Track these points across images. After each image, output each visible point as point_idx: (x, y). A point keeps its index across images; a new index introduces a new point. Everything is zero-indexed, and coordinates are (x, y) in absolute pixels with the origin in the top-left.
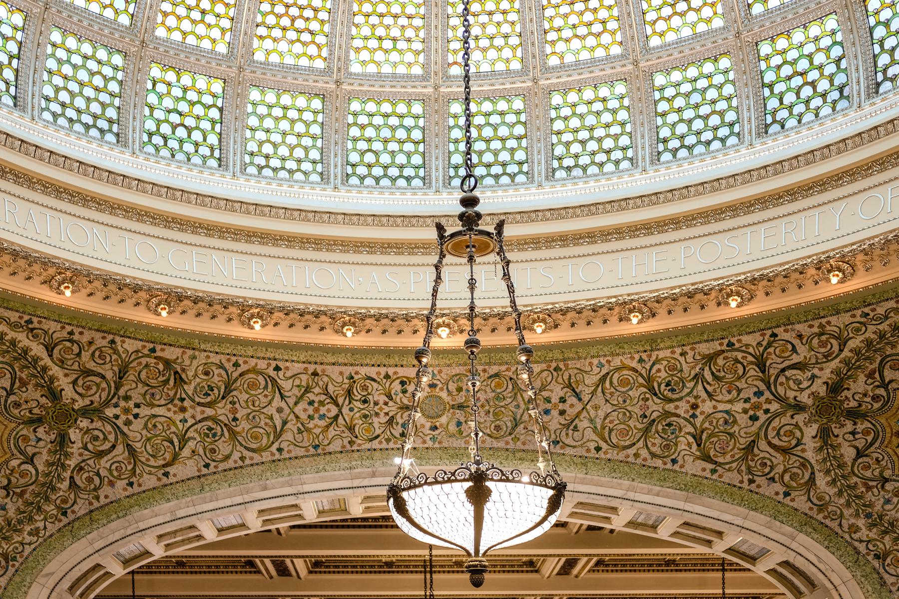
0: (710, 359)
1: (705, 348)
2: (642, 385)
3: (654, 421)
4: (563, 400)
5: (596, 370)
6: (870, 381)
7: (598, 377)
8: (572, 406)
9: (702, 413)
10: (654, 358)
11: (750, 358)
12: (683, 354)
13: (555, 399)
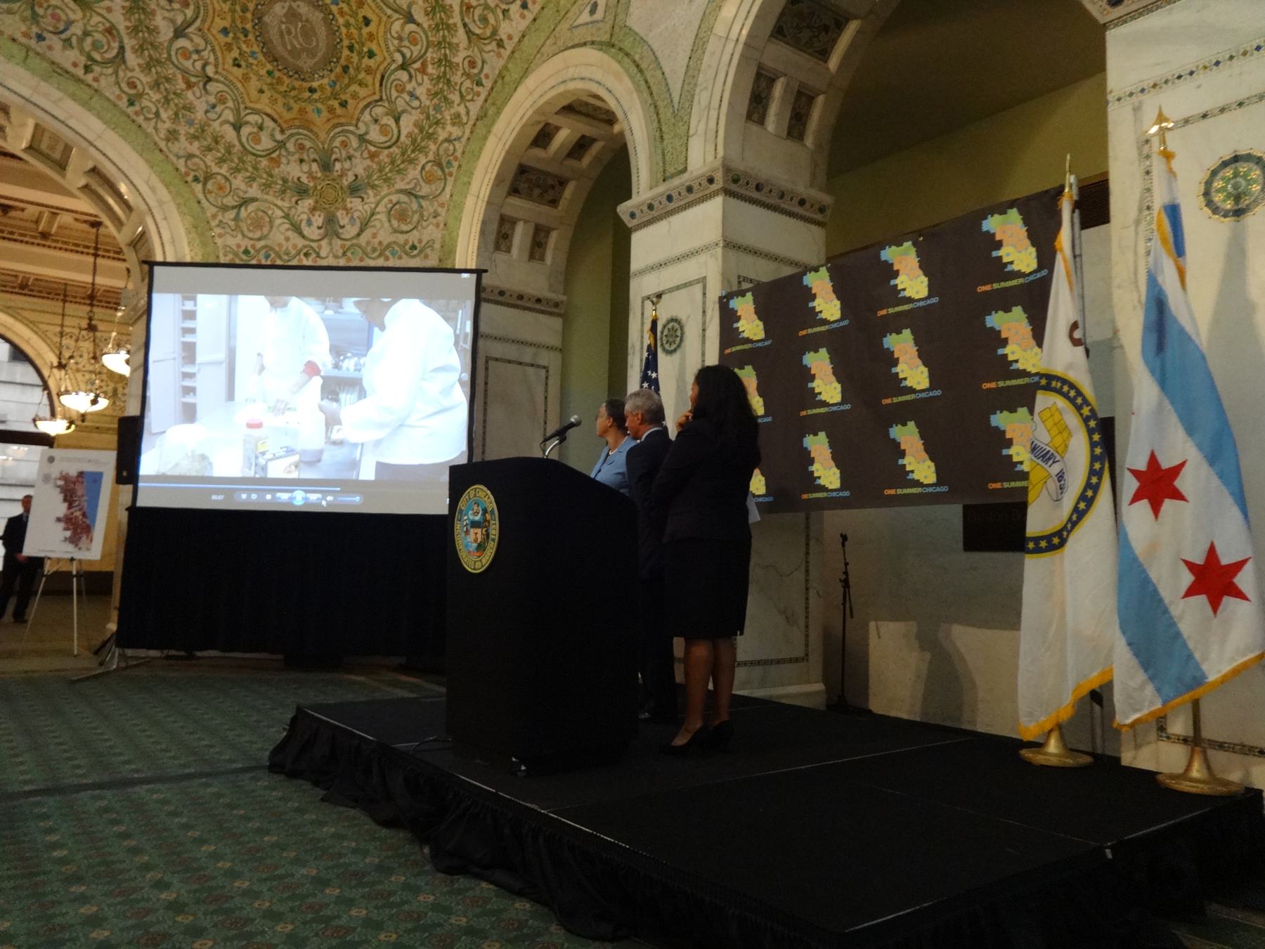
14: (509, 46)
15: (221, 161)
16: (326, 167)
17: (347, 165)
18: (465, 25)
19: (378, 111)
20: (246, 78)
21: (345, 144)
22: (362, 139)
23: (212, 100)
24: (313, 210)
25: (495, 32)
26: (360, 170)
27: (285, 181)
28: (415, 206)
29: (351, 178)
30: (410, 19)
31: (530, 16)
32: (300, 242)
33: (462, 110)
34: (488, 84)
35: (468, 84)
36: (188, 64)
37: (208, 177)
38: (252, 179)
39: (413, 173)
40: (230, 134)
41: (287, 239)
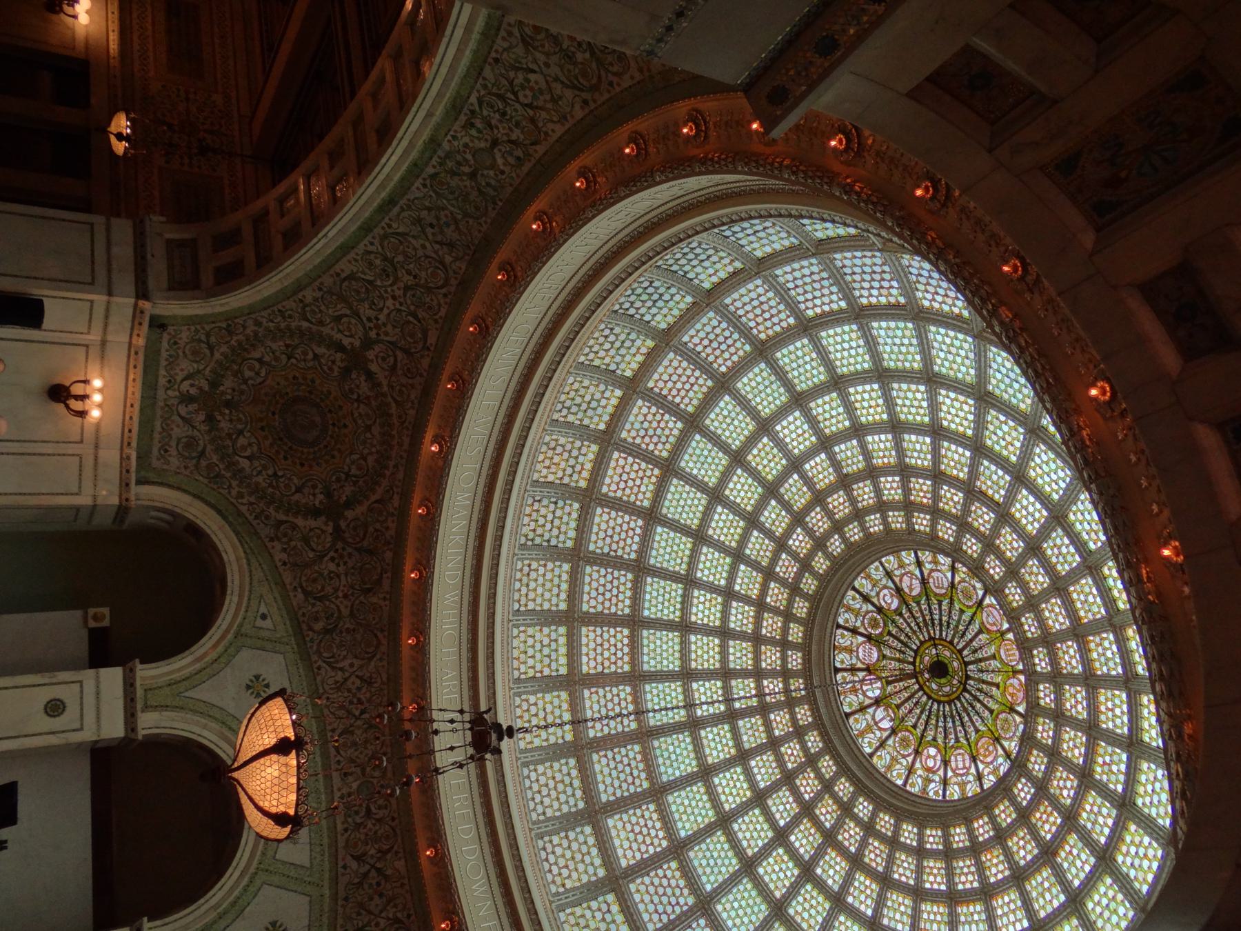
14: (269, 545)
15: (239, 343)
16: (228, 404)
17: (227, 418)
18: (286, 522)
19: (255, 448)
20: (287, 379)
21: (239, 420)
22: (241, 432)
23: (277, 354)
24: (200, 389)
25: (279, 539)
26: (222, 425)
27: (223, 376)
28: (194, 454)
29: (219, 418)
30: (298, 490)
31: (279, 564)
32: (179, 378)
33: (244, 501)
34: (254, 523)
35: (258, 510)
36: (299, 351)
37: (230, 333)
38: (226, 357)
39: (215, 458)
40: (257, 355)
41: (182, 370)
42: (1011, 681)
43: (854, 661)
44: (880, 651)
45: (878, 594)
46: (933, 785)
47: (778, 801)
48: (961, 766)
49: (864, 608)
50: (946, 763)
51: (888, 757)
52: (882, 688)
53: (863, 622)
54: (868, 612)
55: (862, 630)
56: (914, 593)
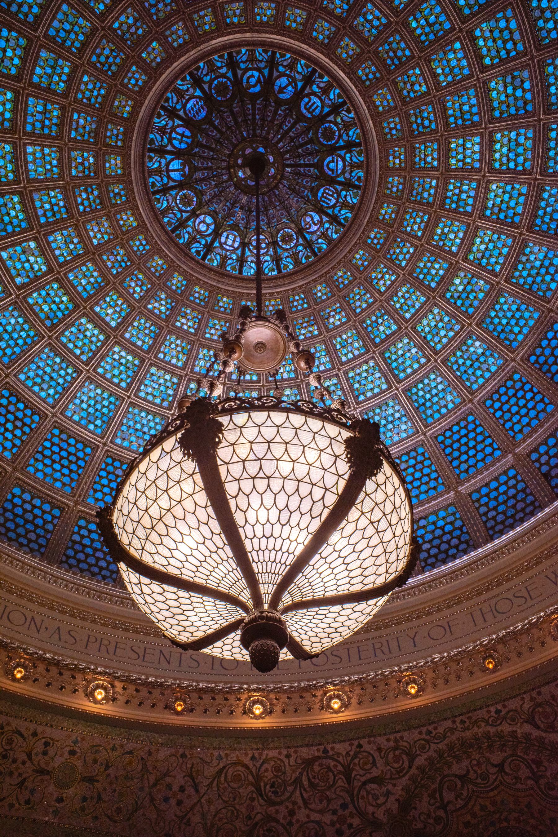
0: (308, 763)
1: (306, 753)
2: (252, 784)
3: (257, 824)
4: (182, 789)
5: (215, 762)
6: (432, 801)
7: (216, 770)
8: (189, 796)
9: (298, 821)
10: (264, 757)
11: (340, 768)
12: (288, 756)
13: (175, 788)
42: (313, 214)
43: (179, 107)
44: (209, 113)
45: (247, 70)
46: (197, 245)
47: (45, 198)
48: (230, 242)
49: (224, 70)
50: (217, 234)
51: (165, 204)
52: (190, 146)
53: (212, 80)
54: (223, 76)
55: (206, 87)
56: (281, 96)
